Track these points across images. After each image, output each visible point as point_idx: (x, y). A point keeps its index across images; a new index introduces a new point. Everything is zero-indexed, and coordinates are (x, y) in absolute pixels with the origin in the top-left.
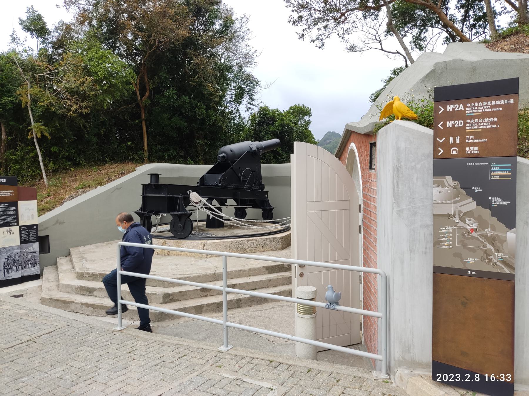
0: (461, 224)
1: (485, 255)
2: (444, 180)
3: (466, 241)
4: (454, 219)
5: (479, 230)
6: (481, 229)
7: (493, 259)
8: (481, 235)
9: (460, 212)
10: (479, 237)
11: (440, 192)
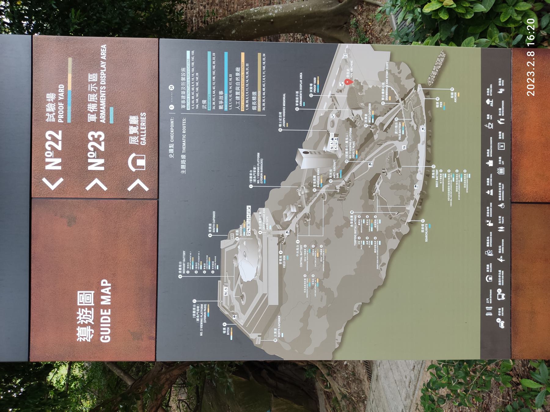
0: (292, 227)
1: (336, 195)
2: (226, 250)
3: (317, 220)
4: (285, 237)
5: (301, 203)
6: (298, 202)
7: (341, 185)
8: (308, 201)
9: (274, 228)
10: (311, 204)
11: (245, 256)
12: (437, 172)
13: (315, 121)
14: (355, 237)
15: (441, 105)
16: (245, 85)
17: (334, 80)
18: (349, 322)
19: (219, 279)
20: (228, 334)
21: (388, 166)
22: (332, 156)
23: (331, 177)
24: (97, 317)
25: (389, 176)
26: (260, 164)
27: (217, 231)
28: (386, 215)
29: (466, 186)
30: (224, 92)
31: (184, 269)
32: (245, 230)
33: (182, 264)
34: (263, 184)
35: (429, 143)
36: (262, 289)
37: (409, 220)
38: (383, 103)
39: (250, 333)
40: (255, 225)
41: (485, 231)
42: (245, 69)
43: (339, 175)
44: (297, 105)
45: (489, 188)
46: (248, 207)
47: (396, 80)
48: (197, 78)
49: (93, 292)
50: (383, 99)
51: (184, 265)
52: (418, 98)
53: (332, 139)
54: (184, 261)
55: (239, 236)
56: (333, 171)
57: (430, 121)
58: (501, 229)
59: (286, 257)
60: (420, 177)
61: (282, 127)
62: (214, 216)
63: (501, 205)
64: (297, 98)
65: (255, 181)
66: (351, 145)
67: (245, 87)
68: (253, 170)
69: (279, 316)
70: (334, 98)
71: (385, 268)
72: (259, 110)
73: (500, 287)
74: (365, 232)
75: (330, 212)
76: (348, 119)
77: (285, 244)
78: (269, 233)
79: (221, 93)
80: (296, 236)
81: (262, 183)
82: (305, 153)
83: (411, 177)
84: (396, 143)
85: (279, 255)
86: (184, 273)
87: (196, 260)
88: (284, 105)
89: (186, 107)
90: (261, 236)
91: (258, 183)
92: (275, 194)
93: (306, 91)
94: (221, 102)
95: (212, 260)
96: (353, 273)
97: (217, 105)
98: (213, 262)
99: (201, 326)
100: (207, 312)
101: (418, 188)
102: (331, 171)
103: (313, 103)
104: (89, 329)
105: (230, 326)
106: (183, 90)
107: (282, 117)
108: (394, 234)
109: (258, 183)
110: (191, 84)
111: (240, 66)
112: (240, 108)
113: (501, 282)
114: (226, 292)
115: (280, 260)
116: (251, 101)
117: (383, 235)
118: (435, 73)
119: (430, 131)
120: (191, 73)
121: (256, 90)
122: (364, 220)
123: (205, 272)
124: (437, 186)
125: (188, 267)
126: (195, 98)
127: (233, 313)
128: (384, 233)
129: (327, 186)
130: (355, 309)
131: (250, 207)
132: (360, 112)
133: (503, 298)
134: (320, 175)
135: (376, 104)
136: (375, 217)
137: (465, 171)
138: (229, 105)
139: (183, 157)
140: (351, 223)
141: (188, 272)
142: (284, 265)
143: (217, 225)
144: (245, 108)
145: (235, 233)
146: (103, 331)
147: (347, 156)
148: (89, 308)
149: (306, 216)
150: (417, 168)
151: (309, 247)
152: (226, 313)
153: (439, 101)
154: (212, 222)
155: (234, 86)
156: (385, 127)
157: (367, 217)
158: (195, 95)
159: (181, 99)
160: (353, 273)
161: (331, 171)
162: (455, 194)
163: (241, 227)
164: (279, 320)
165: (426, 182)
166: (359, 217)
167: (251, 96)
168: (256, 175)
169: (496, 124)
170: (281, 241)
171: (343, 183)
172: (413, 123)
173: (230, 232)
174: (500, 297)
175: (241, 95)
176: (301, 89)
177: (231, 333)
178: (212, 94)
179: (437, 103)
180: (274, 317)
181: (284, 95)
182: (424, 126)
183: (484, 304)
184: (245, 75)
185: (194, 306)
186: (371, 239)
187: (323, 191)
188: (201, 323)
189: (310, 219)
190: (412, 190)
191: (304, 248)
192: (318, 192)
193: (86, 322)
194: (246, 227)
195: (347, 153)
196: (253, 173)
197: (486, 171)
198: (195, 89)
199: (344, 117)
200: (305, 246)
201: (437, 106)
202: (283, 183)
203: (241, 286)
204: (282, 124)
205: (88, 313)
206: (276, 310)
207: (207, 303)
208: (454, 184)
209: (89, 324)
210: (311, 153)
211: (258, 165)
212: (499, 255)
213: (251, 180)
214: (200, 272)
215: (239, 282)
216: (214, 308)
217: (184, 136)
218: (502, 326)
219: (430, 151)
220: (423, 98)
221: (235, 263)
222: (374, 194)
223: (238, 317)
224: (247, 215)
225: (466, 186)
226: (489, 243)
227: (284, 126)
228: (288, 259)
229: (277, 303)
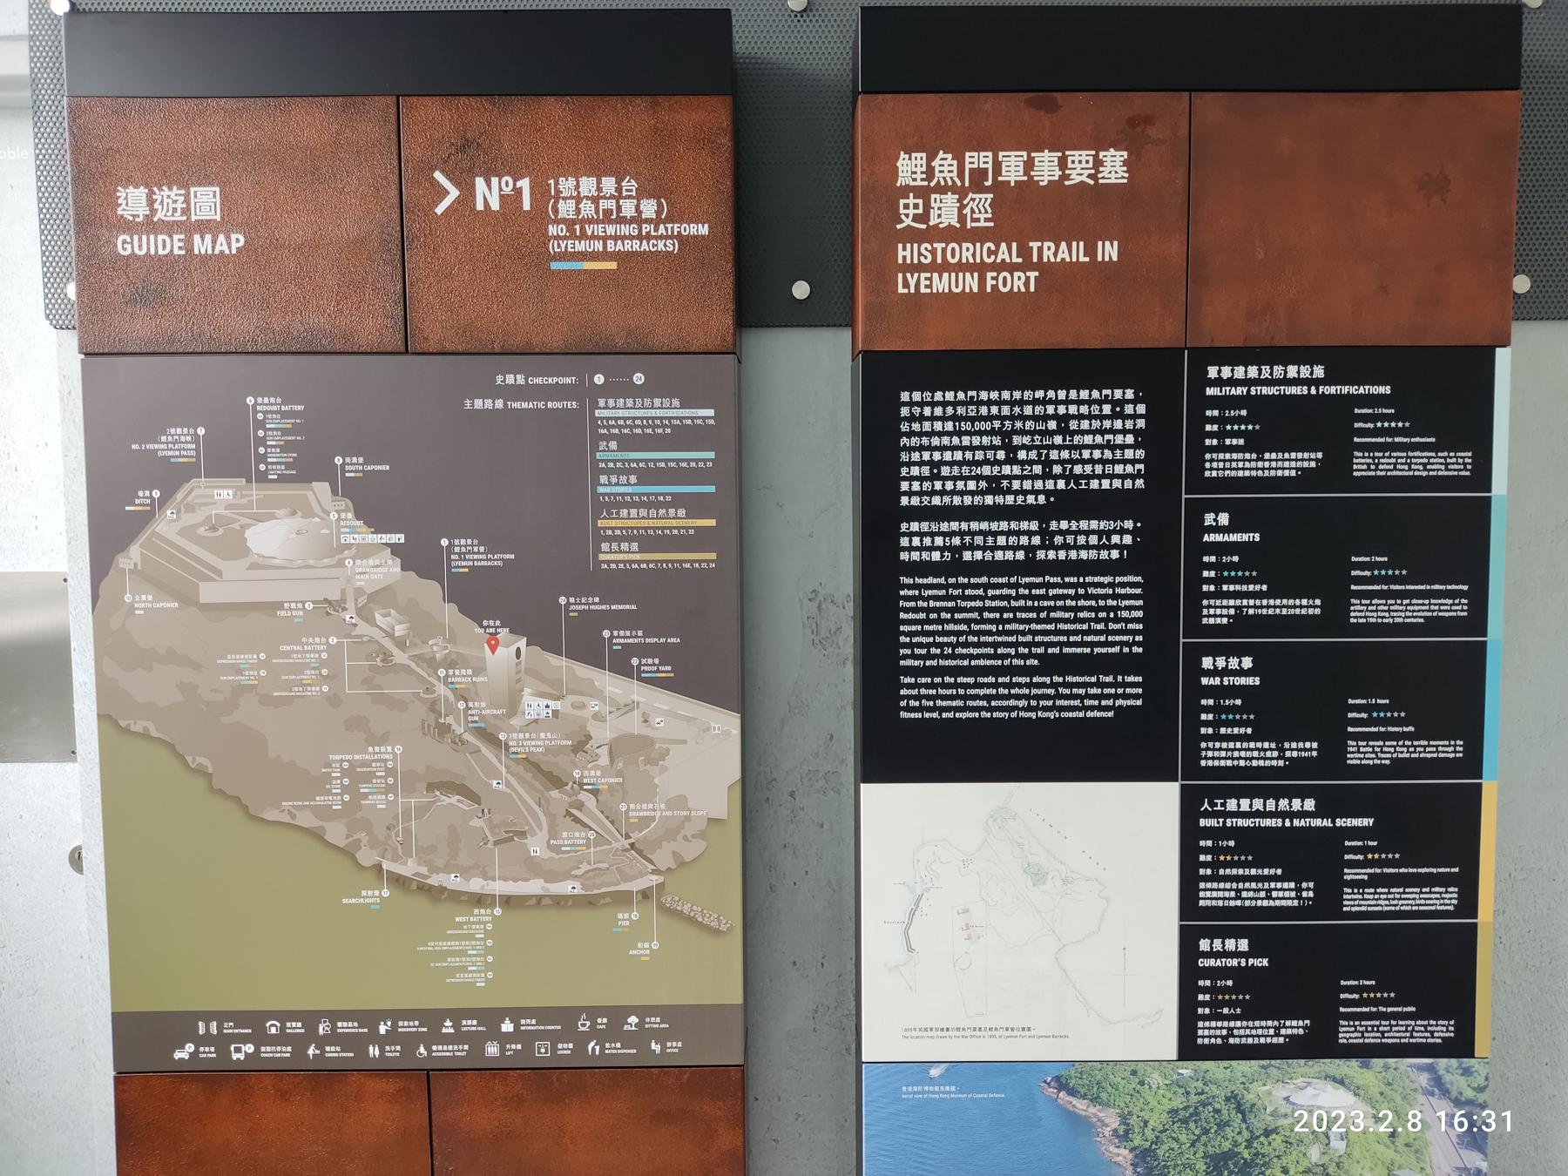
0: (363, 628)
2: (310, 494)
5: (414, 645)
7: (455, 726)
8: (418, 658)
9: (359, 591)
10: (413, 665)
11: (298, 533)
13: (583, 671)
14: (349, 757)
18: (171, 747)
19: (249, 481)
22: (513, 706)
24: (170, 228)
29: (460, 978)
32: (353, 530)
35: (545, 901)
38: (623, 807)
40: (364, 551)
41: (369, 1018)
45: (457, 1026)
47: (672, 831)
49: (218, 218)
50: (632, 806)
51: (275, 408)
52: (636, 878)
56: (482, 708)
58: (374, 1051)
60: (476, 885)
62: (380, 468)
63: (422, 1050)
65: (457, 549)
66: (537, 744)
67: (646, 529)
70: (630, 707)
71: (286, 818)
73: (257, 1050)
76: (589, 737)
79: (633, 479)
84: (543, 835)
85: (304, 603)
87: (285, 432)
90: (341, 564)
92: (431, 590)
93: (643, 651)
95: (288, 466)
101: (453, 881)
103: (620, 665)
104: (143, 211)
105: (152, 505)
110: (647, 418)
113: (267, 1051)
114: (224, 493)
120: (670, 418)
121: (641, 551)
123: (262, 450)
126: (620, 427)
128: (358, 816)
129: (452, 698)
130: (200, 760)
132: (604, 760)
133: (235, 1056)
134: (474, 683)
135: (620, 792)
138: (609, 495)
139: (499, 404)
141: (260, 416)
142: (282, 613)
144: (605, 529)
145: (346, 510)
146: (140, 239)
148: (186, 211)
149: (387, 656)
151: (323, 663)
152: (179, 496)
153: (630, 919)
154: (365, 463)
155: (638, 505)
156: (575, 812)
158: (627, 426)
159: (616, 397)
161: (483, 704)
162: (442, 955)
163: (359, 523)
165: (465, 898)
166: (390, 764)
167: (630, 539)
169: (588, 1037)
170: (334, 606)
172: (585, 867)
174: (238, 1050)
178: (630, 461)
180: (175, 595)
182: (578, 891)
183: (221, 1017)
184: (671, 528)
186: (345, 789)
187: (442, 690)
190: (448, 869)
191: (320, 652)
193: (156, 206)
195: (521, 736)
197: (490, 1017)
199: (593, 728)
200: (324, 656)
201: (620, 916)
203: (236, 526)
205: (175, 210)
206: (188, 599)
208: (463, 953)
209: (153, 211)
212: (320, 1047)
214: (262, 442)
215: (244, 521)
216: (187, 472)
217: (541, 405)
218: (178, 1055)
220: (636, 886)
221: (281, 512)
225: (460, 978)
226: (344, 1027)
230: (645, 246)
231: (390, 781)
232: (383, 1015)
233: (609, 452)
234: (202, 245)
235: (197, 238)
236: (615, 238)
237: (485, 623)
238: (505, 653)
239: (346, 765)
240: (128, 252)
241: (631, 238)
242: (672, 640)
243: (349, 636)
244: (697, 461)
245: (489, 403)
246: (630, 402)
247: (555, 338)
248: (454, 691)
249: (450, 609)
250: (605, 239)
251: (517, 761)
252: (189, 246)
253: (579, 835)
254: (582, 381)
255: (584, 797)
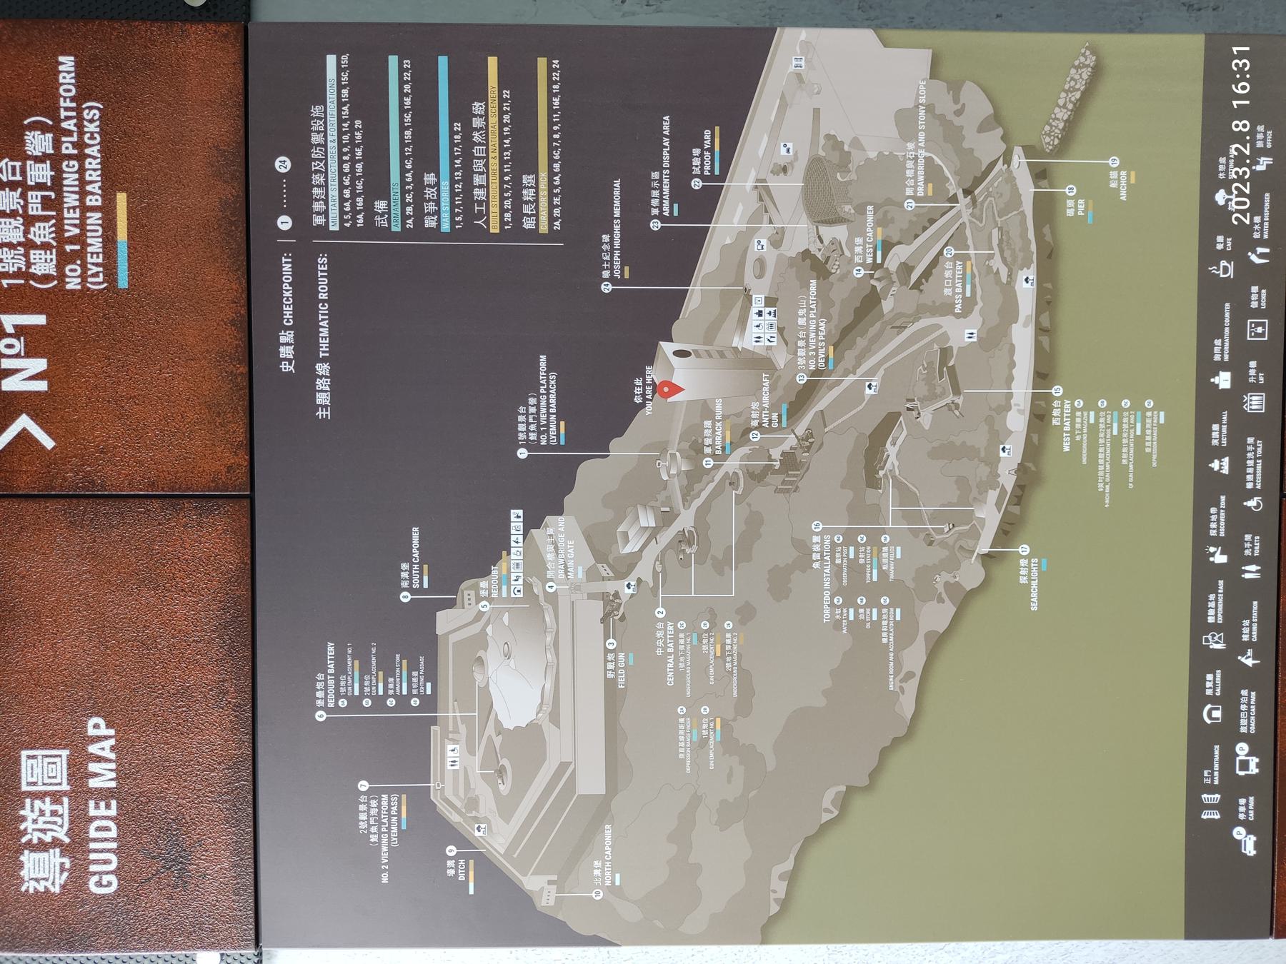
0: (644, 570)
2: (453, 638)
4: (624, 599)
5: (669, 500)
6: (662, 496)
7: (786, 447)
8: (688, 495)
9: (592, 574)
10: (697, 503)
12: (1067, 406)
13: (709, 260)
15: (1081, 208)
16: (501, 156)
17: (766, 138)
18: (808, 842)
19: (434, 721)
20: (462, 878)
21: (922, 390)
22: (758, 363)
23: (755, 423)
25: (926, 419)
26: (548, 389)
27: (426, 585)
28: (915, 533)
29: (1152, 447)
30: (438, 176)
31: (331, 696)
33: (326, 681)
34: (558, 448)
35: (1046, 323)
36: (557, 748)
37: (984, 547)
38: (910, 205)
39: (525, 875)
40: (535, 565)
41: (1204, 577)
42: (500, 107)
43: (780, 417)
44: (655, 212)
46: (514, 513)
47: (947, 133)
48: (359, 136)
50: (909, 192)
51: (331, 682)
52: (1015, 189)
53: (760, 314)
54: (331, 671)
55: (489, 599)
56: (761, 407)
57: (1050, 256)
59: (626, 657)
60: (1017, 421)
61: (612, 280)
62: (416, 541)
64: (655, 193)
65: (533, 437)
66: (814, 328)
68: (527, 405)
69: (608, 827)
70: (763, 192)
71: (912, 686)
72: (544, 228)
74: (853, 584)
75: (753, 525)
76: (806, 254)
77: (623, 618)
78: (576, 588)
79: (429, 178)
80: (655, 594)
81: (553, 442)
82: (679, 353)
83: (989, 421)
84: (947, 323)
85: (607, 651)
86: (331, 705)
87: (365, 670)
88: (617, 213)
89: (327, 223)
90: (553, 599)
91: (543, 442)
93: (681, 171)
94: (431, 207)
95: (413, 666)
96: (821, 702)
97: (420, 215)
98: (415, 674)
99: (385, 857)
100: (399, 816)
101: (1011, 455)
102: (755, 405)
103: (702, 205)
105: (466, 857)
106: (316, 172)
107: (612, 250)
108: (941, 589)
109: (543, 442)
110: (341, 154)
111: (484, 98)
112: (487, 222)
114: (452, 757)
115: (610, 666)
116: (518, 201)
117: (907, 593)
118: (1062, 115)
119: (1049, 286)
120: (340, 121)
122: (852, 549)
124: (1066, 449)
125: (343, 690)
126: (354, 195)
127: (476, 819)
128: (911, 585)
129: (744, 450)
131: (520, 512)
132: (840, 232)
134: (724, 418)
135: (887, 209)
136: (885, 538)
137: (1149, 403)
138: (453, 215)
139: (323, 369)
140: (816, 556)
141: (343, 703)
142: (621, 681)
143: (426, 567)
145: (476, 588)
147: (801, 361)
149: (684, 538)
150: (1010, 396)
151: (693, 628)
152: (454, 818)
153: (1076, 198)
155: (468, 158)
156: (915, 276)
157: (862, 538)
158: (353, 185)
159: (310, 199)
160: (821, 702)
161: (755, 405)
162: (1118, 470)
163: (495, 573)
164: (608, 838)
165: (1035, 438)
166: (839, 539)
167: (518, 187)
168: (537, 419)
171: (791, 441)
172: (997, 263)
173: (463, 586)
175: (489, 183)
176: (666, 164)
177: (471, 874)
178: (403, 183)
179: (1070, 203)
181: (617, 184)
183: (1195, 787)
184: (501, 125)
185: (363, 798)
186: (873, 603)
187: (733, 463)
188: (385, 849)
189: (695, 547)
190: (993, 462)
191: (677, 631)
192: (716, 467)
194: (509, 572)
195: (801, 352)
196: (527, 414)
198: (353, 169)
199: (793, 248)
200: (682, 625)
201: (1070, 213)
202: (615, 443)
203: (498, 741)
204: (612, 269)
206: (600, 810)
207: (399, 791)
208: (1116, 442)
210: (698, 355)
211: (542, 391)
213: (522, 436)
214: (379, 702)
216: (421, 805)
217: (324, 309)
219: (1047, 347)
220: (1027, 188)
221: (479, 679)
222: (881, 473)
223: (490, 828)
224: (513, 538)
227: (617, 275)
228: (631, 662)
229: (601, 790)
230: (93, 151)
231: (862, 538)
232: (1200, 558)
233: (391, 212)
234: (103, 776)
235: (93, 783)
236: (83, 193)
237: (638, 400)
238: (681, 373)
239: (838, 600)
240: (113, 878)
241: (82, 171)
242: (666, 128)
243: (654, 591)
244: (402, 83)
245: (323, 384)
246: (317, 179)
247: (226, 284)
248: (735, 446)
249: (619, 448)
250: (84, 209)
251: (837, 361)
252: (104, 795)
253: (950, 270)
254: (287, 248)
255: (892, 263)
